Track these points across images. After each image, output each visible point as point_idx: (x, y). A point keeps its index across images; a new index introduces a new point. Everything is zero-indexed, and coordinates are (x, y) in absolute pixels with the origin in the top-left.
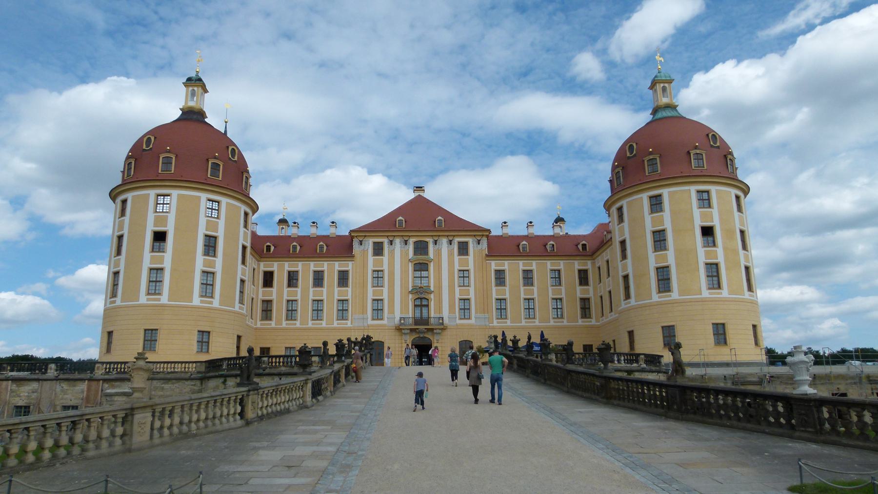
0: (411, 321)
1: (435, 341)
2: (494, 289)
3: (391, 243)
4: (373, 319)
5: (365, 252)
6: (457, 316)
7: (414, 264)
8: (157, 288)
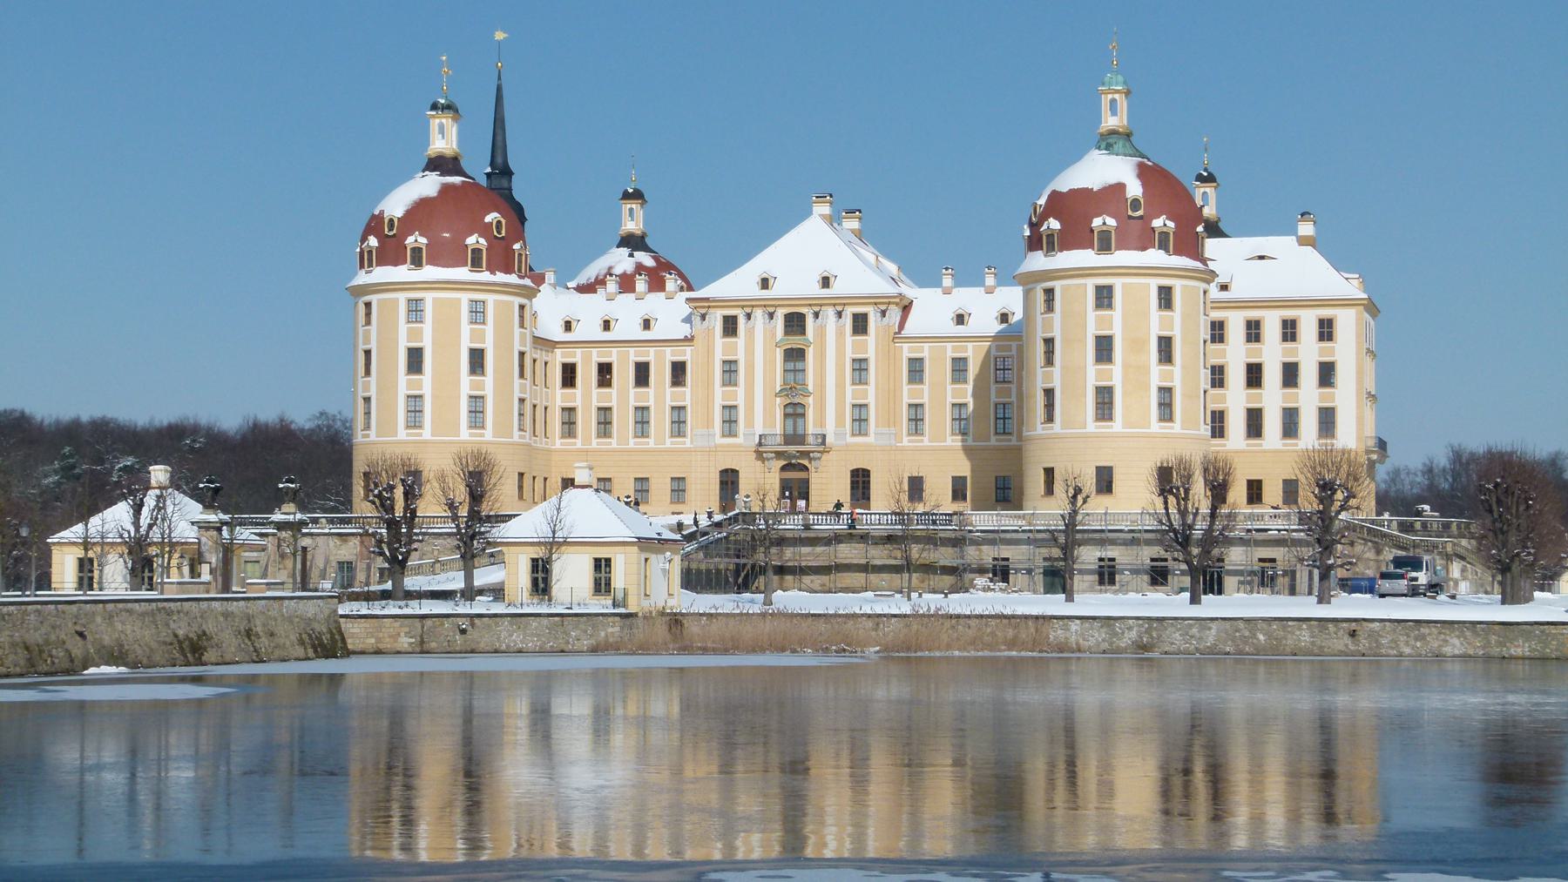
0: (779, 440)
1: (814, 470)
2: (906, 388)
3: (749, 316)
4: (723, 436)
5: (710, 331)
6: (848, 432)
7: (785, 350)
8: (417, 419)
